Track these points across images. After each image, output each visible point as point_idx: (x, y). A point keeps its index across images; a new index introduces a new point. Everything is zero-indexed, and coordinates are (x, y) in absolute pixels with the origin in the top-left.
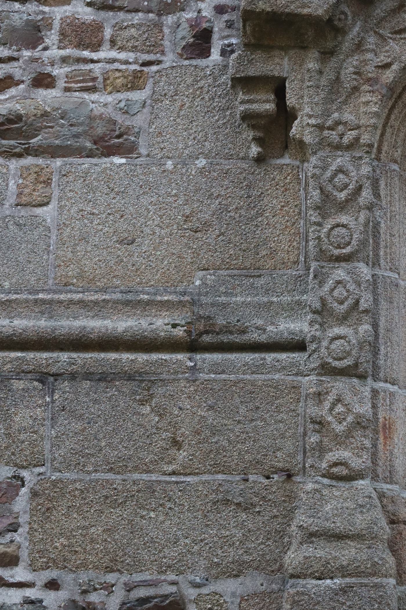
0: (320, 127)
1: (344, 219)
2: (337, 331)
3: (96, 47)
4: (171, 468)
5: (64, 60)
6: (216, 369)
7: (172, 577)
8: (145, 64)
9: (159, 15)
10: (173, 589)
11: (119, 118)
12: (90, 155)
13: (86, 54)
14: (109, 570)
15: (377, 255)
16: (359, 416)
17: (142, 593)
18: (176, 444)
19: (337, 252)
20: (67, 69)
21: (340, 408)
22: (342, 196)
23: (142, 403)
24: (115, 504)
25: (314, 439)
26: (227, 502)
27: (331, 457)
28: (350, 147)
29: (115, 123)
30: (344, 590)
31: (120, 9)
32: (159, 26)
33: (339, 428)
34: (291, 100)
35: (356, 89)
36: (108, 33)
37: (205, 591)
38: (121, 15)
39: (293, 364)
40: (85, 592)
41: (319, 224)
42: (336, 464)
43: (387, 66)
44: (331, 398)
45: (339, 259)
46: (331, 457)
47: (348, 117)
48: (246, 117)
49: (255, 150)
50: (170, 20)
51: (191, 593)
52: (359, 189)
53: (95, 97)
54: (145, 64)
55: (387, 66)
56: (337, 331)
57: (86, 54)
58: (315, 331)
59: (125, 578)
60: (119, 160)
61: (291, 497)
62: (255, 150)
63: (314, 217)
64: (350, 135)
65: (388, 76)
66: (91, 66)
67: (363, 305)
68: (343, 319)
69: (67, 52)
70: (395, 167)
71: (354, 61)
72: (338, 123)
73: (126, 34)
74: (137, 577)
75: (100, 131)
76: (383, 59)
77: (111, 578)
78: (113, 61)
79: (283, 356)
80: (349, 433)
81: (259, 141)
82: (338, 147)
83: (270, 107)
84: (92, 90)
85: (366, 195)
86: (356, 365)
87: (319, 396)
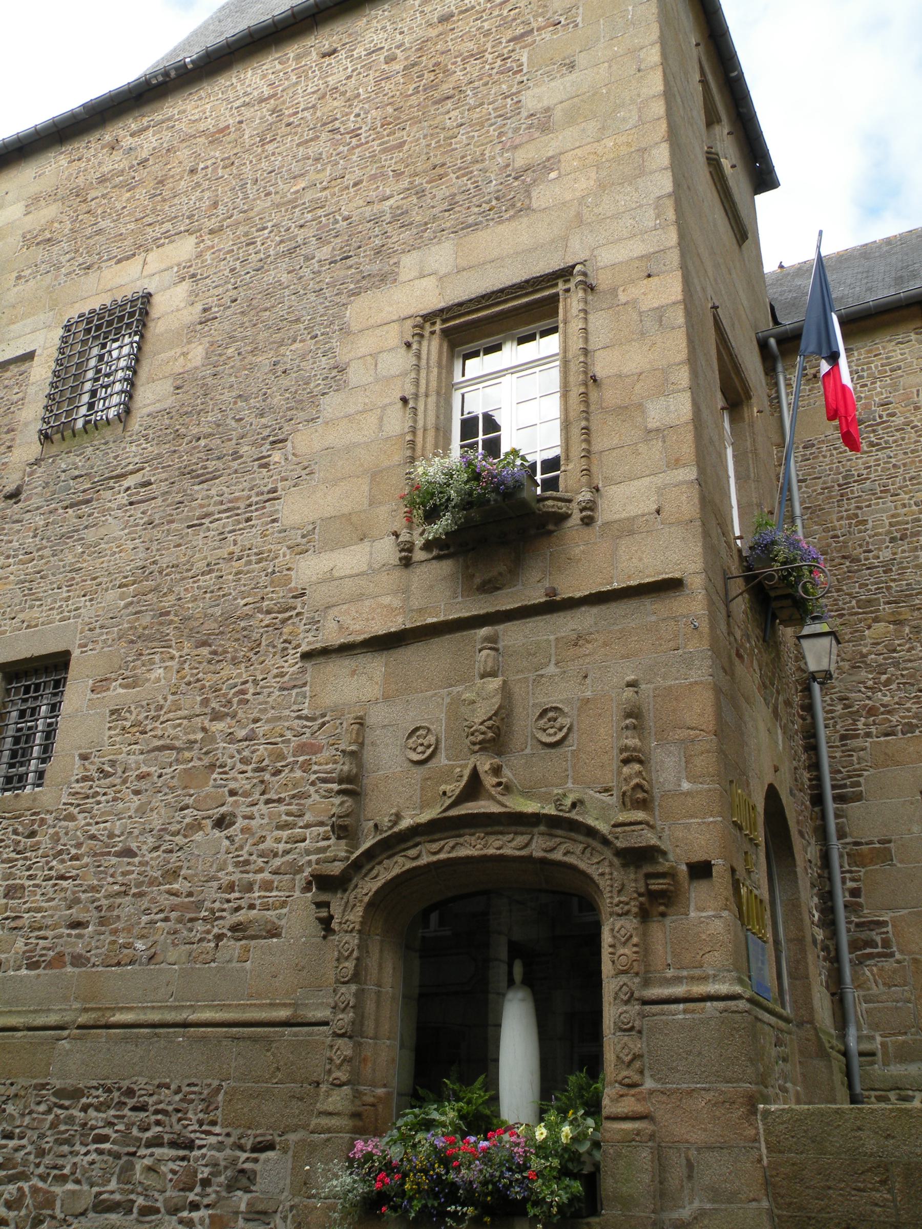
0: (340, 923)
1: (346, 964)
2: (341, 1016)
3: (271, 891)
4: (275, 1081)
5: (259, 897)
6: (296, 1035)
7: (271, 1132)
8: (287, 897)
9: (294, 875)
10: (271, 1137)
11: (276, 921)
12: (265, 938)
13: (267, 894)
14: (249, 1128)
15: (366, 979)
16: (346, 1056)
17: (259, 1139)
18: (278, 1069)
19: (342, 980)
20: (260, 901)
21: (339, 1053)
22: (346, 954)
23: (268, 1050)
24: (254, 1098)
25: (328, 1067)
26: (294, 1097)
27: (334, 1075)
28: (351, 931)
29: (274, 923)
30: (328, 1140)
31: (280, 874)
32: (294, 879)
33: (338, 1062)
34: (332, 913)
35: (355, 905)
36: (276, 884)
37: (283, 1138)
38: (281, 876)
39: (324, 1032)
40: (239, 1139)
41: (337, 967)
42: (335, 1079)
43: (367, 894)
44: (336, 1047)
45: (344, 983)
46: (334, 1075)
47: (352, 918)
48: (317, 918)
49: (323, 933)
50: (298, 877)
51: (278, 1139)
52: (353, 950)
53: (269, 913)
54: (287, 897)
55: (367, 894)
56: (341, 1016)
57: (267, 894)
58: (331, 1017)
59: (254, 1132)
60: (275, 940)
61: (318, 1095)
62: (323, 933)
63: (335, 964)
64: (351, 926)
65: (366, 899)
66: (266, 900)
67: (351, 1004)
68: (343, 1010)
69: (263, 894)
70: (378, 937)
71: (354, 893)
72: (347, 921)
73: (281, 884)
74: (258, 1132)
75: (269, 928)
76: (365, 891)
77: (249, 1132)
78: (276, 896)
79: (321, 1028)
80: (341, 1065)
81: (324, 929)
82: (346, 932)
83: (325, 914)
84: (268, 909)
85: (355, 954)
86: (346, 1032)
87: (331, 1047)
